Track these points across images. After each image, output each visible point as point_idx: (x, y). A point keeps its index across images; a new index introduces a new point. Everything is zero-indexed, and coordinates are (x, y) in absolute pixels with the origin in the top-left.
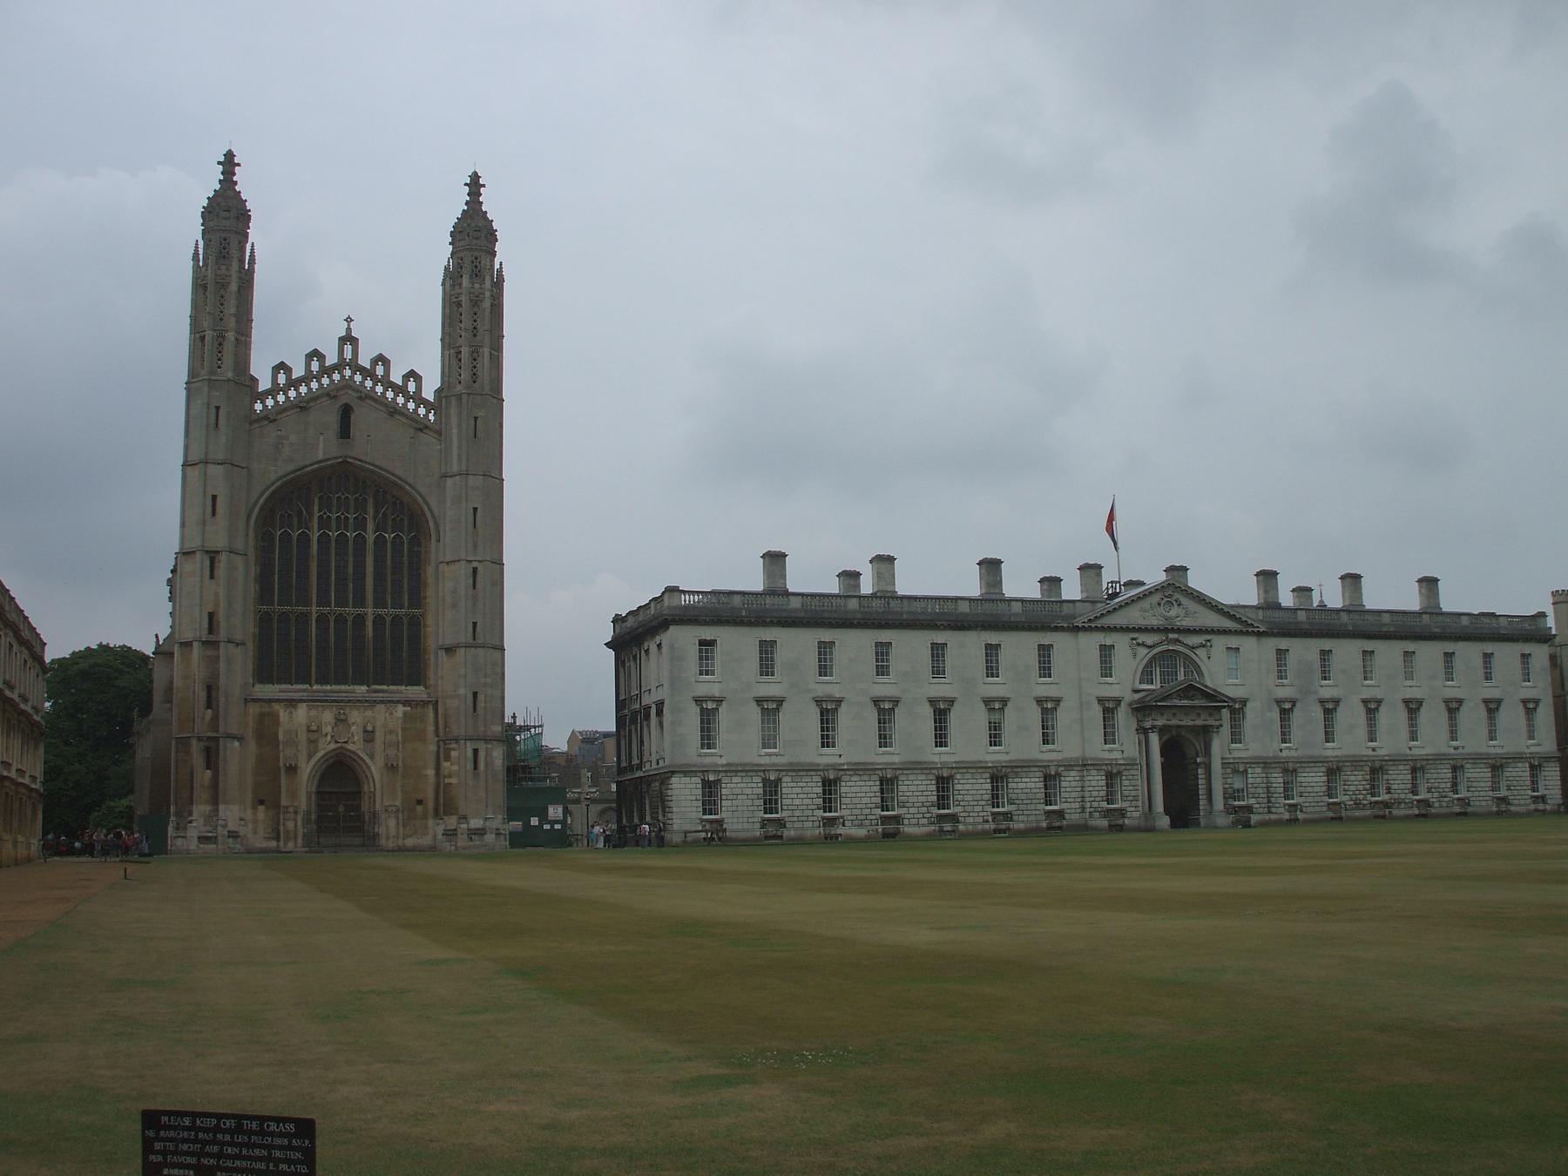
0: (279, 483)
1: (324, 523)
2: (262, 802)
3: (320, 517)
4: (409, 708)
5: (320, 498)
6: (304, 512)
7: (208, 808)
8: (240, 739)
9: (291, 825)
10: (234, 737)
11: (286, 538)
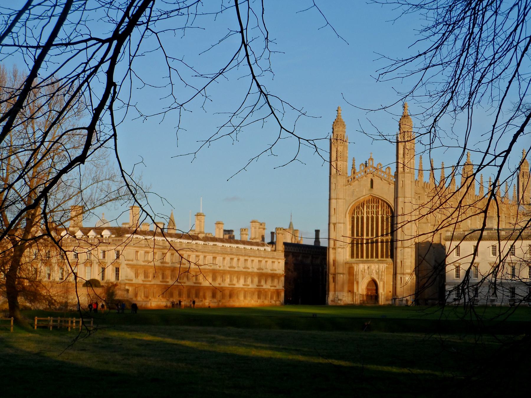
0: (353, 203)
1: (368, 213)
2: (350, 291)
3: (367, 211)
4: (387, 265)
5: (367, 206)
6: (363, 210)
7: (334, 293)
8: (343, 274)
9: (357, 297)
10: (340, 274)
11: (358, 218)
